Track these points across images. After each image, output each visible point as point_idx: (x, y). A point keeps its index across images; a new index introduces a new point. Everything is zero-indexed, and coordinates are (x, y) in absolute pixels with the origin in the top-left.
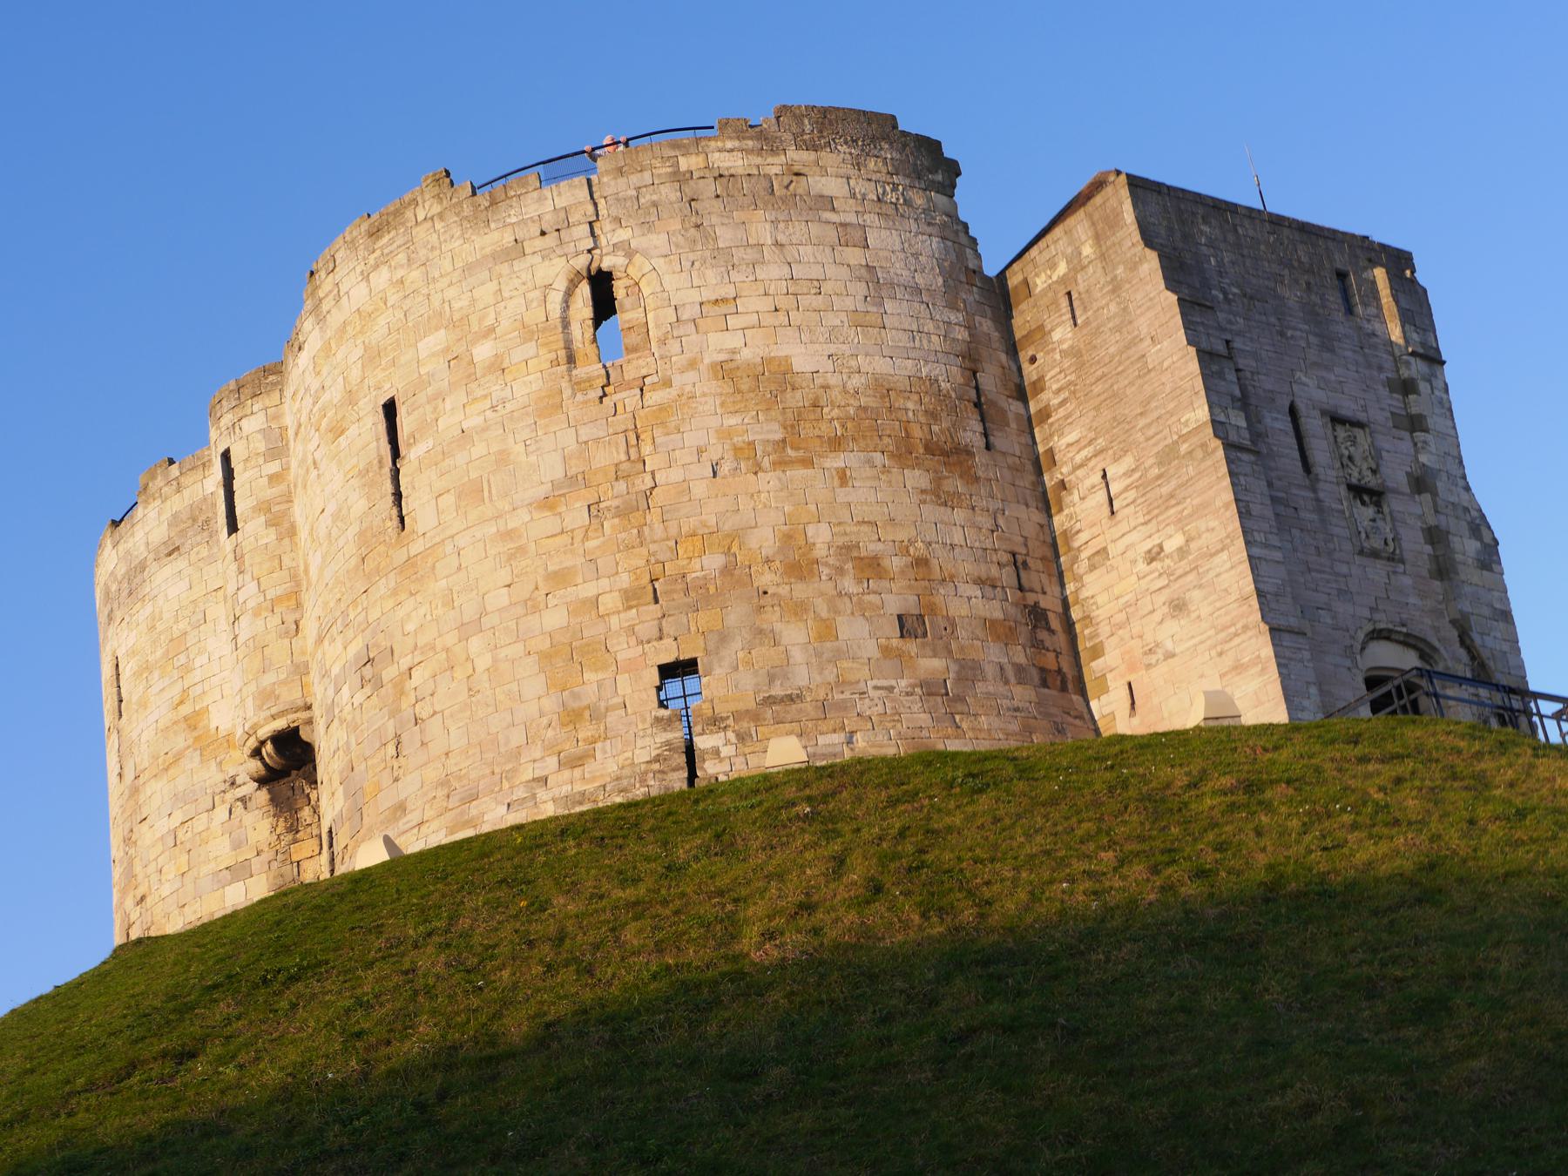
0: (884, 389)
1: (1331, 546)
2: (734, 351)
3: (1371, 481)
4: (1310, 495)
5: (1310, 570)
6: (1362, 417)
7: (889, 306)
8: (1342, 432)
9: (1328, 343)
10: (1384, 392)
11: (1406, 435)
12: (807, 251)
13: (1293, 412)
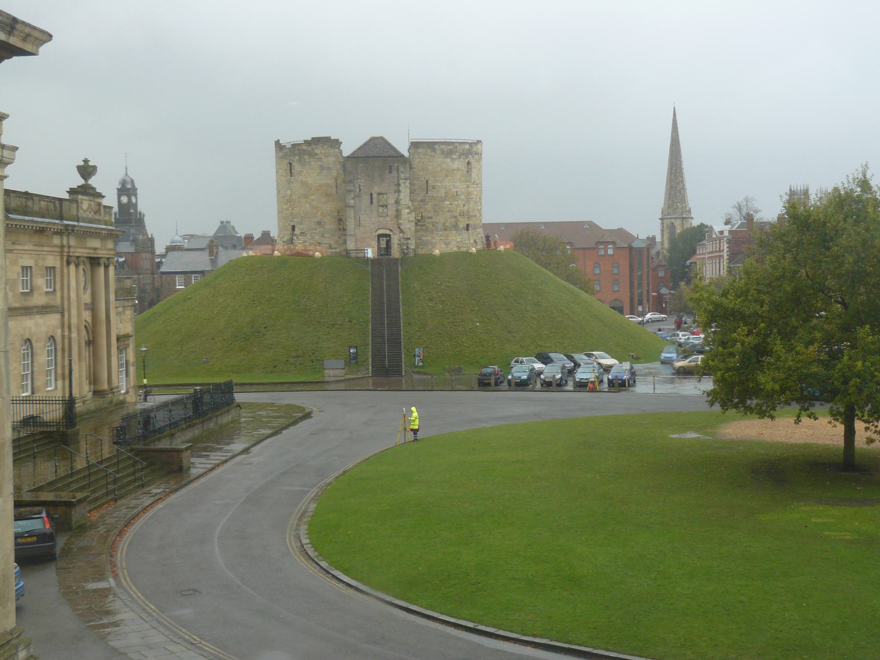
0: (320, 185)
12: (313, 163)
13: (371, 194)
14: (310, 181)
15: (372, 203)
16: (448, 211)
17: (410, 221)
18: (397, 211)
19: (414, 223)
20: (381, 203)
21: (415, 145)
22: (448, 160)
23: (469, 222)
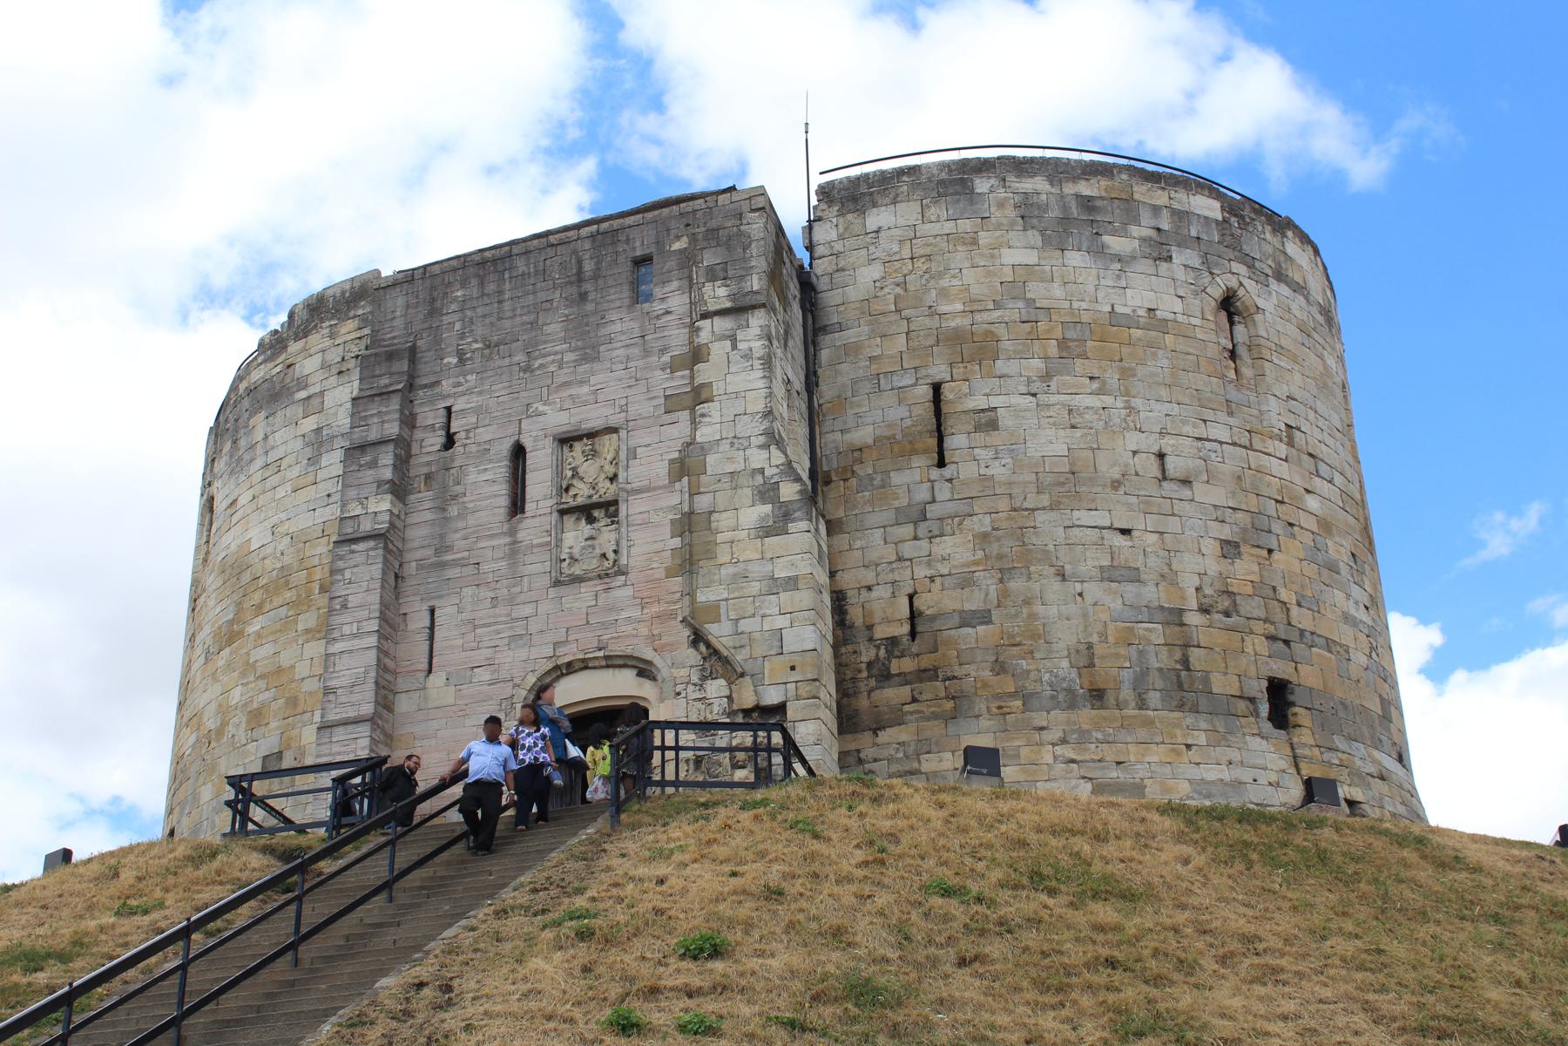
1: (518, 589)
2: (228, 547)
3: (607, 490)
4: (508, 540)
5: (475, 627)
6: (614, 421)
7: (325, 461)
8: (578, 446)
9: (590, 355)
10: (659, 375)
11: (684, 415)
13: (519, 452)
14: (257, 535)
15: (517, 505)
16: (1110, 575)
17: (776, 585)
18: (689, 524)
19: (804, 598)
20: (582, 494)
21: (846, 197)
22: (1075, 258)
23: (1281, 669)
